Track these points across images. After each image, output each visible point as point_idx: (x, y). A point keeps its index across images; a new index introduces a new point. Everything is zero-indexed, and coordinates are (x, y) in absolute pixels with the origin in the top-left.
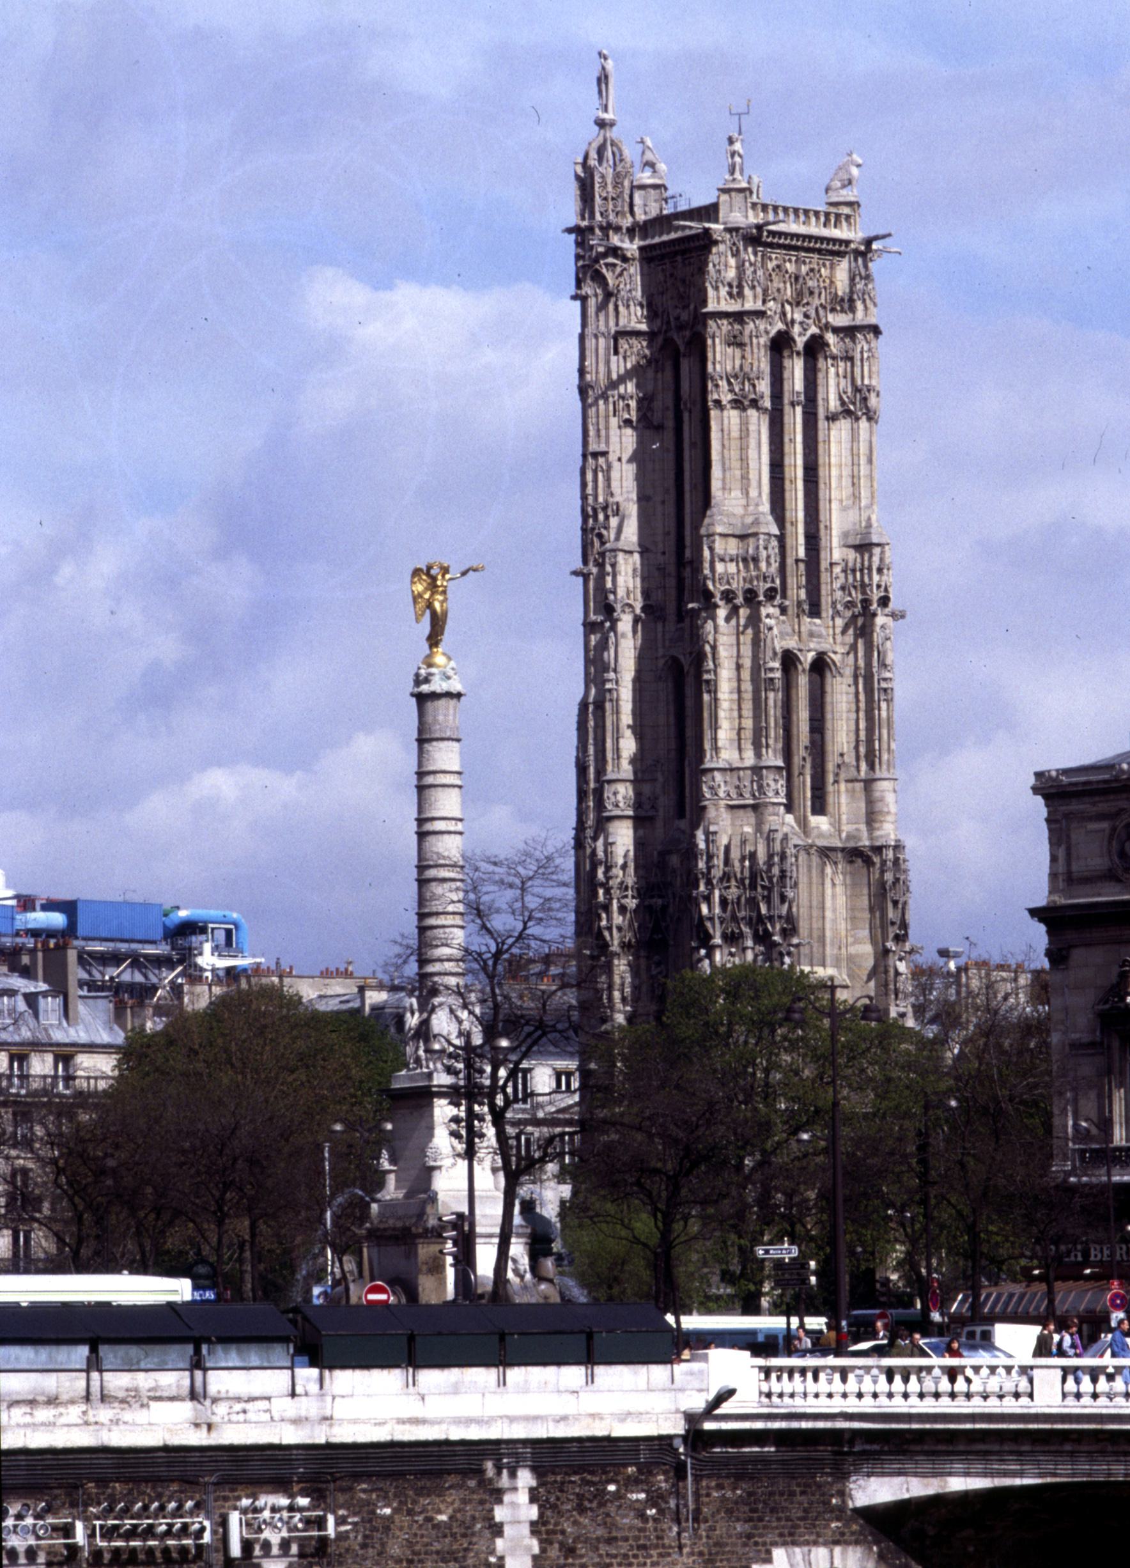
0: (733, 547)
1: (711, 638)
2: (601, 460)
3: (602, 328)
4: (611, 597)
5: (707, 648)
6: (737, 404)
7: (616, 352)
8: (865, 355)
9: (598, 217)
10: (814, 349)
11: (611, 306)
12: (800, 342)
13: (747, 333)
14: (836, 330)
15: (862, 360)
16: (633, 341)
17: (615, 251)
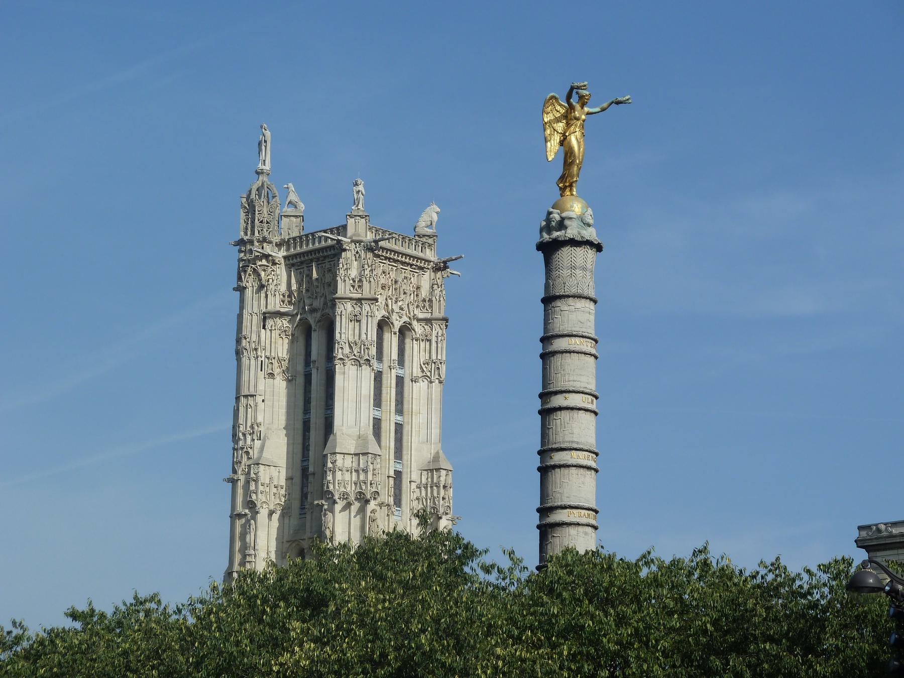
0: (348, 462)
1: (330, 525)
3: (256, 310)
4: (254, 497)
5: (328, 533)
6: (358, 363)
7: (264, 328)
8: (440, 338)
9: (256, 232)
10: (404, 331)
12: (397, 325)
13: (364, 313)
14: (419, 320)
15: (437, 342)
16: (278, 321)
17: (267, 257)
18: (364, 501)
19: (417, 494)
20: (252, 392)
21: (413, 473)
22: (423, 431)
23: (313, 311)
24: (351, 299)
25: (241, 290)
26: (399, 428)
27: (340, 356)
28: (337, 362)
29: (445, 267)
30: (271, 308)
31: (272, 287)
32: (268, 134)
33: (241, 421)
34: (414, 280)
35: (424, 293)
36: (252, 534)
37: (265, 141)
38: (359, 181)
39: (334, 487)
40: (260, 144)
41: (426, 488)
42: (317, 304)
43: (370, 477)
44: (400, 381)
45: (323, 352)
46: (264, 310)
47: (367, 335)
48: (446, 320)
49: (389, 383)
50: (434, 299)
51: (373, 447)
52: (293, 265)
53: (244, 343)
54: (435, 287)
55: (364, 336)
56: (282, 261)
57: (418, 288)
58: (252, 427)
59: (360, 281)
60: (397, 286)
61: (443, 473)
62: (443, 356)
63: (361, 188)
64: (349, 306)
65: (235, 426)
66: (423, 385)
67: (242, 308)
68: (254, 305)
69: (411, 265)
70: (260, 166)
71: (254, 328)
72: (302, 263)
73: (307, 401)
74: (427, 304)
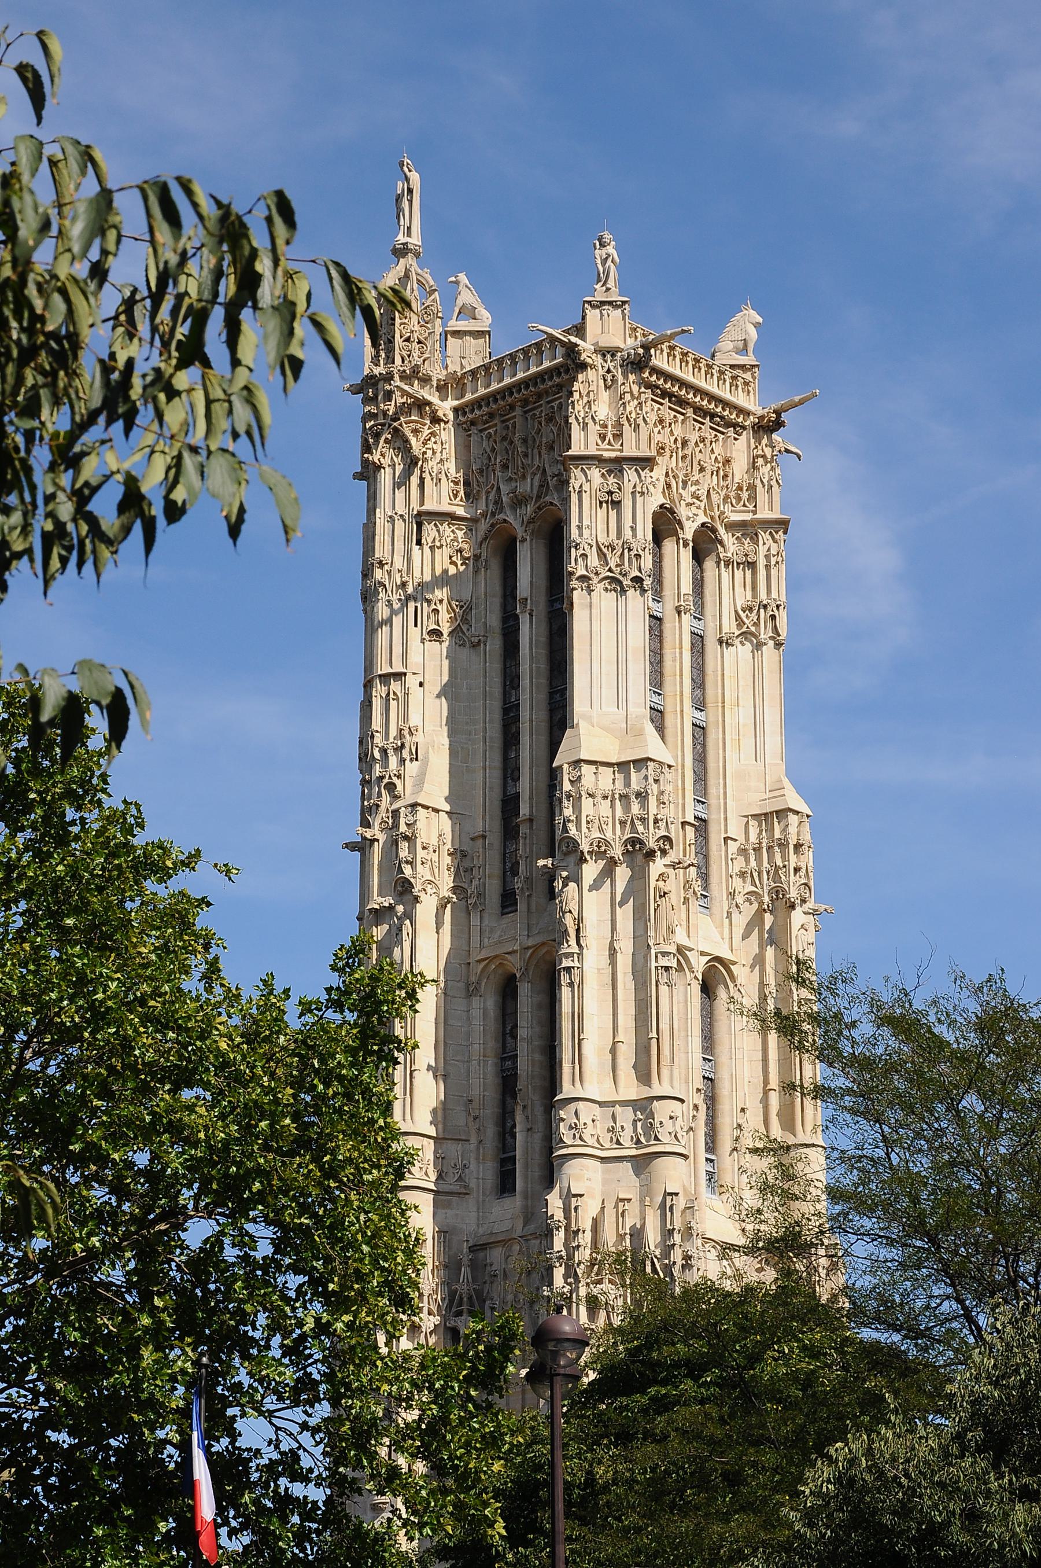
0: (606, 780)
1: (573, 906)
2: (395, 686)
3: (401, 509)
4: (407, 870)
5: (569, 921)
6: (616, 585)
7: (419, 543)
8: (773, 561)
9: (398, 360)
10: (704, 545)
11: (415, 480)
13: (628, 488)
14: (731, 527)
15: (768, 567)
16: (446, 529)
17: (421, 405)
18: (639, 853)
19: (739, 864)
20: (398, 668)
21: (732, 823)
22: (748, 742)
23: (518, 502)
24: (599, 460)
25: (369, 472)
26: (700, 729)
27: (581, 571)
28: (574, 583)
29: (778, 425)
30: (429, 506)
31: (432, 465)
32: (415, 177)
33: (376, 723)
34: (718, 448)
35: (739, 469)
36: (407, 945)
37: (410, 191)
38: (607, 236)
39: (579, 828)
40: (399, 199)
41: (757, 850)
42: (525, 487)
43: (653, 808)
44: (698, 641)
45: (542, 583)
46: (415, 507)
47: (633, 529)
48: (783, 524)
49: (679, 633)
50: (758, 482)
51: (654, 747)
52: (473, 423)
53: (378, 574)
54: (760, 461)
55: (628, 533)
56: (451, 416)
57: (728, 461)
58: (400, 735)
59: (619, 425)
60: (688, 452)
61: (793, 819)
62: (780, 593)
63: (611, 250)
64: (595, 474)
65: (365, 738)
66: (743, 651)
67: (371, 511)
68: (393, 502)
69: (713, 416)
70: (401, 238)
71: (399, 545)
72: (491, 415)
73: (510, 680)
74: (745, 495)
